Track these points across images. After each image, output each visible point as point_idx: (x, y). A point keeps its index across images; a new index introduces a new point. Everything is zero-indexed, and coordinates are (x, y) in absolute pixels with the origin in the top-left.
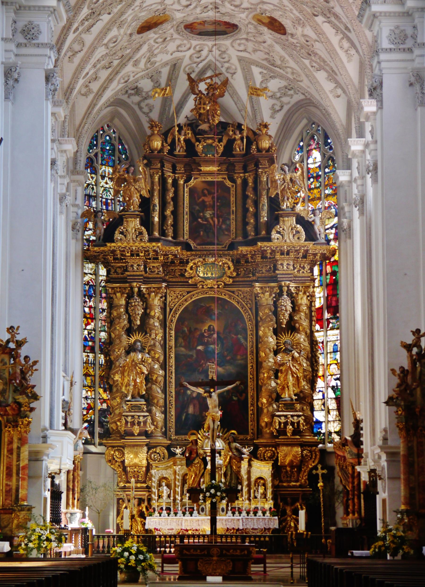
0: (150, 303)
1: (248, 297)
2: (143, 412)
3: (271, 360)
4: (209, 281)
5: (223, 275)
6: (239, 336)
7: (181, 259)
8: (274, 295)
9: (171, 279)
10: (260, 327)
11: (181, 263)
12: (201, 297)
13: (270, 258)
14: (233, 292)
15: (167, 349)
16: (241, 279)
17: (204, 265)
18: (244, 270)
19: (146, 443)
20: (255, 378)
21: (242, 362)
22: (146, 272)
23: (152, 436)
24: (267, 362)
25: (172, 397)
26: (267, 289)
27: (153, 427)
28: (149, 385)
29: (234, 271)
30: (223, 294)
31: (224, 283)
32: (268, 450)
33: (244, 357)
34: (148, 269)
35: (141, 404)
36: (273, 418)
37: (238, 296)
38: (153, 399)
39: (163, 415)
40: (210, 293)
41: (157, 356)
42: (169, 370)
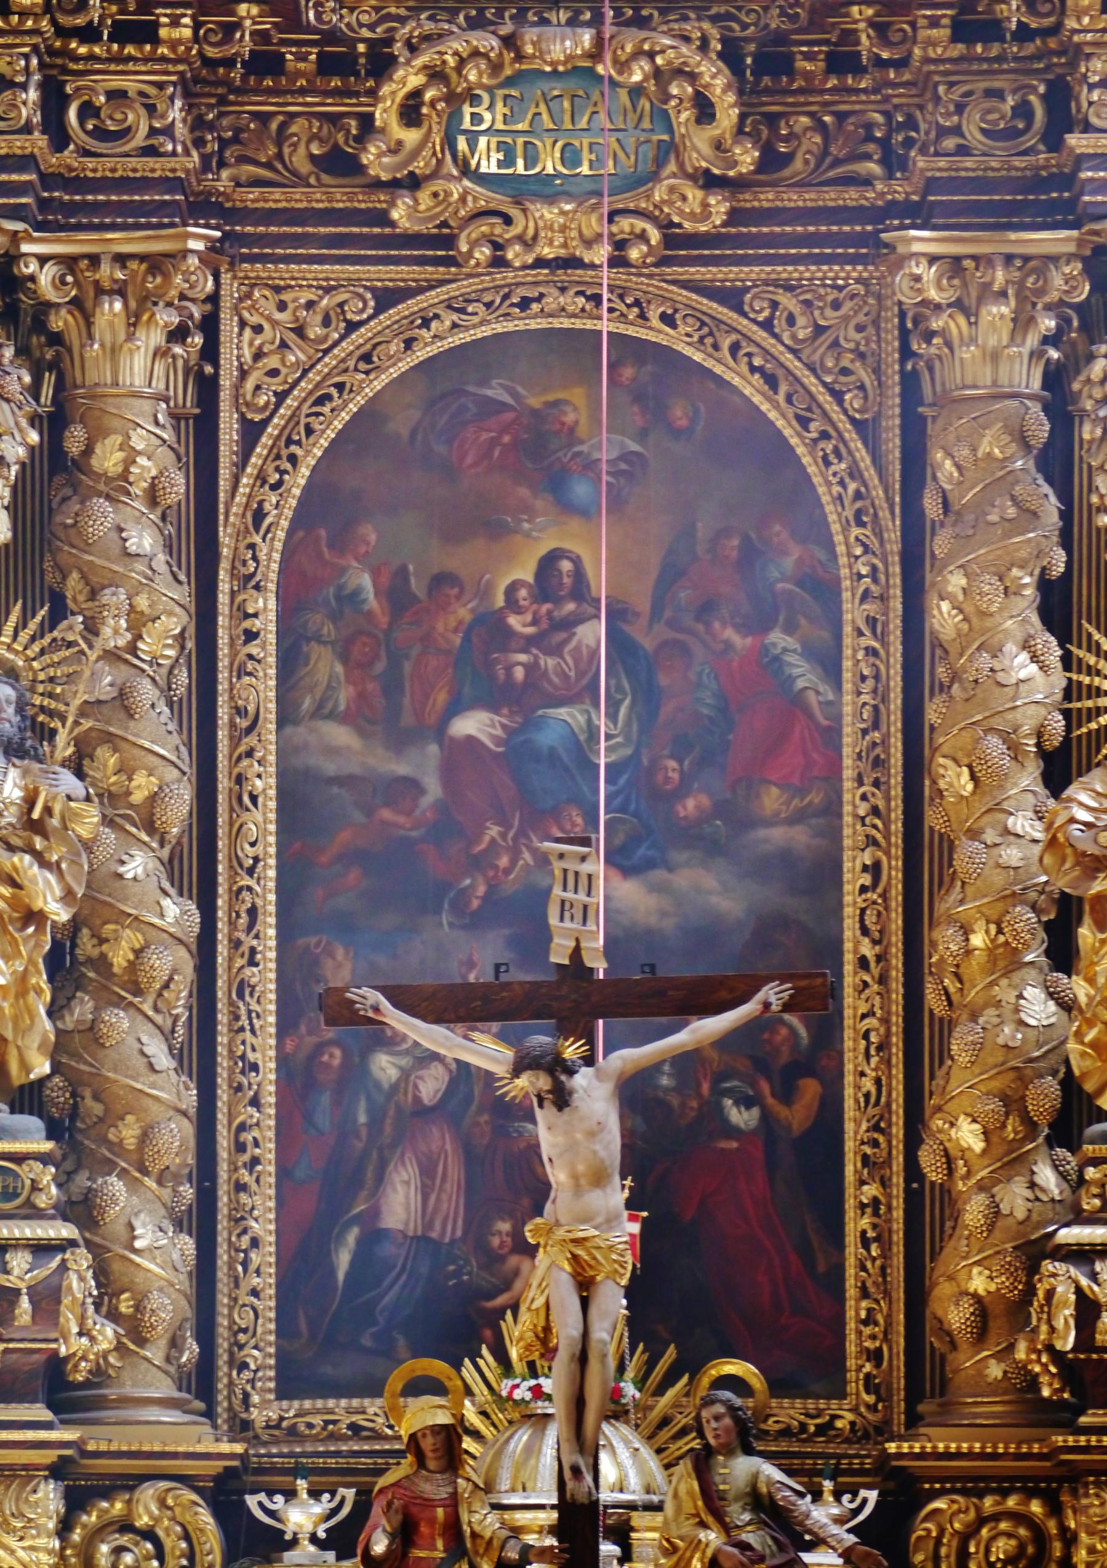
0: (92, 377)
1: (850, 337)
2: (32, 1213)
3: (1023, 823)
4: (548, 213)
5: (660, 163)
6: (778, 638)
7: (331, 36)
8: (1048, 323)
9: (254, 193)
10: (940, 566)
11: (327, 65)
12: (481, 333)
13: (1024, 33)
14: (732, 298)
15: (222, 734)
16: (793, 199)
17: (509, 82)
18: (821, 127)
19: (49, 1456)
20: (897, 961)
21: (799, 837)
22: (60, 138)
23: (101, 1403)
24: (990, 836)
25: (255, 1102)
26: (1000, 276)
27: (107, 1333)
28: (82, 1008)
29: (740, 131)
30: (654, 314)
31: (666, 225)
32: (996, 1518)
33: (815, 797)
34: (72, 114)
35: (19, 1158)
36: (1033, 1269)
37: (767, 325)
38: (112, 1117)
39: (188, 1244)
41: (142, 786)
42: (236, 894)
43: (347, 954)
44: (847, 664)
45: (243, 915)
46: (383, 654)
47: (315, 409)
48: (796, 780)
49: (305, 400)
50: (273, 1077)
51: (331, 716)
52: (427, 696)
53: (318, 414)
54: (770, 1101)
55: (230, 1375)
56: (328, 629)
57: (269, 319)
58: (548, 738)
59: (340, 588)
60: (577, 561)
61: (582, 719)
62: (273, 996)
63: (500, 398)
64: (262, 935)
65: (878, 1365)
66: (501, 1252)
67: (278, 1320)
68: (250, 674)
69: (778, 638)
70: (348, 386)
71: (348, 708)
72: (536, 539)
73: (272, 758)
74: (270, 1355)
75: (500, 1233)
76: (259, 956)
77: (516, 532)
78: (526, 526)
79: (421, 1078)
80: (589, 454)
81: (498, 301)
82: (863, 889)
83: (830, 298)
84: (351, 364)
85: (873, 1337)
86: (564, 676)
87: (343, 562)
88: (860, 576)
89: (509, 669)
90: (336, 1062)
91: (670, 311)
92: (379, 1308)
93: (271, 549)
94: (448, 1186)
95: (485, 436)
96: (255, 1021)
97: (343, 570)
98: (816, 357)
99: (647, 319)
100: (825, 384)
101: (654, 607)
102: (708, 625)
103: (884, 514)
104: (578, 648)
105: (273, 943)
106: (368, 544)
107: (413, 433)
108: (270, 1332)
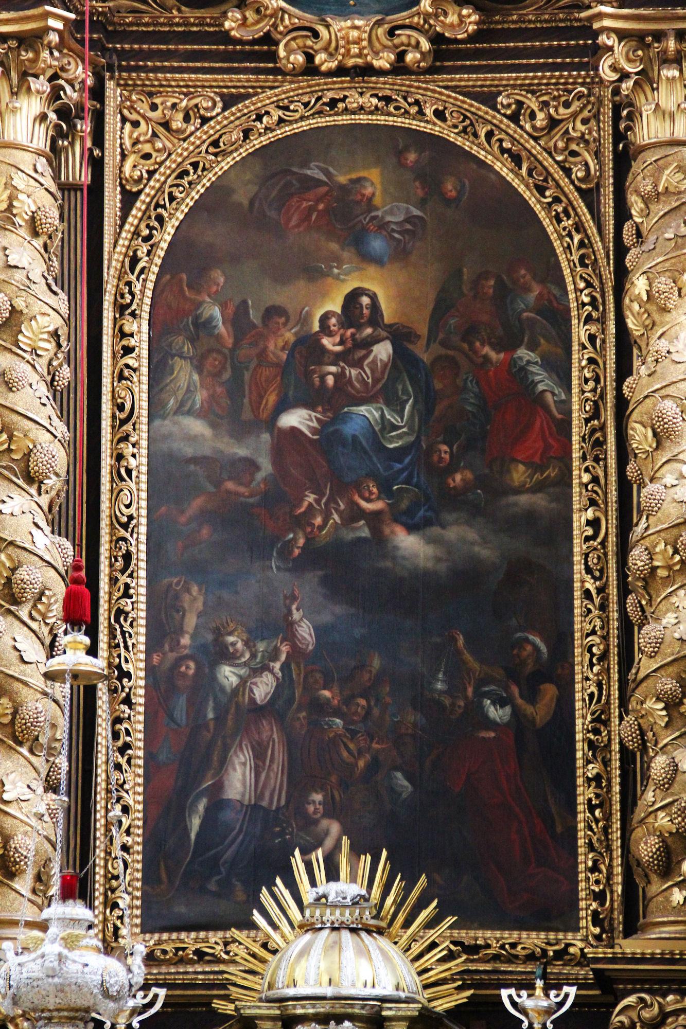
6: (523, 353)
12: (304, 126)
14: (489, 99)
21: (539, 501)
30: (429, 111)
33: (552, 472)
37: (514, 118)
40: (355, 100)
43: (200, 590)
44: (575, 373)
45: (120, 559)
46: (228, 366)
47: (178, 181)
48: (537, 459)
49: (170, 176)
50: (142, 683)
51: (189, 413)
52: (262, 397)
53: (178, 186)
54: (520, 701)
55: (105, 913)
56: (187, 348)
57: (144, 117)
58: (351, 428)
59: (197, 317)
60: (373, 297)
61: (377, 415)
62: (143, 622)
63: (316, 176)
64: (135, 575)
65: (602, 904)
66: (315, 817)
67: (144, 870)
68: (127, 379)
69: (523, 353)
70: (201, 165)
71: (202, 407)
72: (343, 281)
73: (144, 443)
74: (137, 898)
75: (314, 802)
76: (132, 591)
77: (328, 276)
78: (336, 271)
79: (255, 684)
80: (383, 217)
81: (313, 101)
82: (587, 539)
83: (563, 99)
84: (204, 148)
85: (597, 882)
86: (364, 382)
87: (199, 298)
88: (584, 304)
89: (323, 378)
90: (191, 672)
91: (441, 108)
92: (222, 861)
93: (144, 287)
94: (275, 766)
95: (305, 204)
96: (128, 639)
97: (199, 304)
98: (552, 144)
99: (424, 114)
100: (557, 162)
101: (430, 331)
102: (471, 344)
103: (602, 262)
104: (374, 361)
105: (143, 582)
106: (218, 285)
107: (252, 203)
108: (138, 880)
